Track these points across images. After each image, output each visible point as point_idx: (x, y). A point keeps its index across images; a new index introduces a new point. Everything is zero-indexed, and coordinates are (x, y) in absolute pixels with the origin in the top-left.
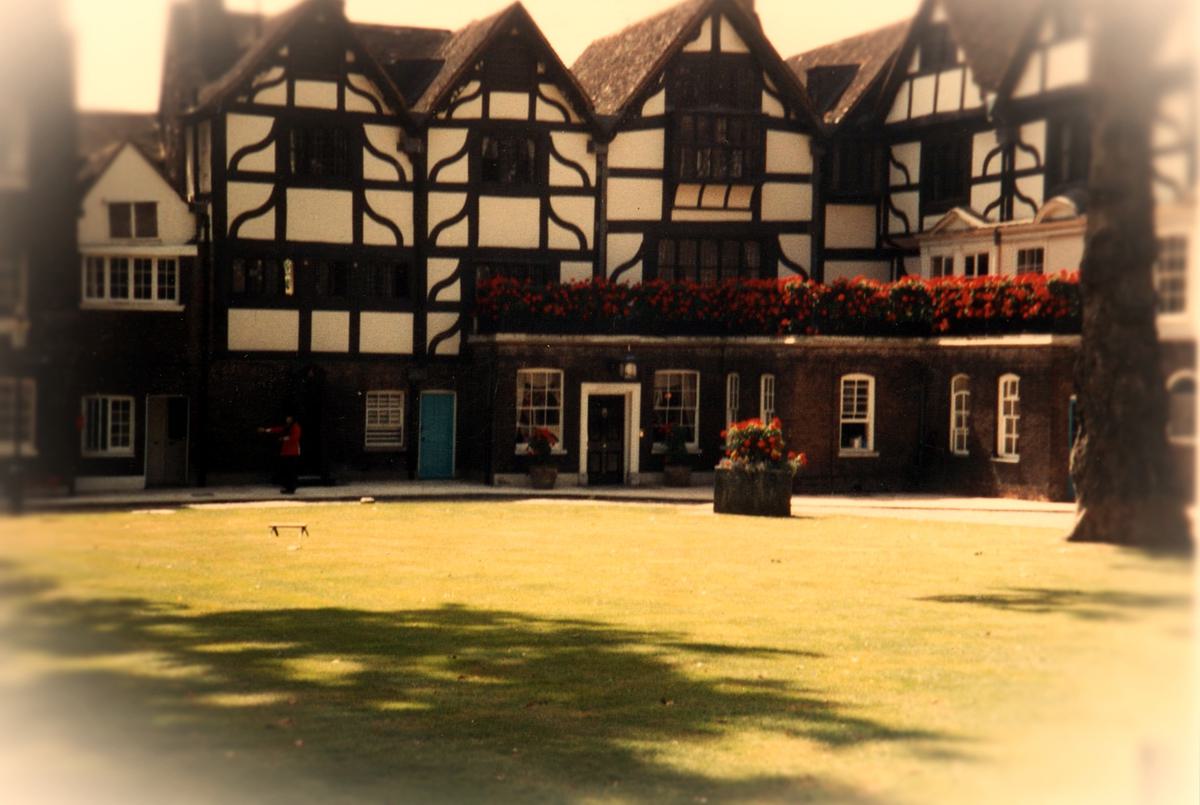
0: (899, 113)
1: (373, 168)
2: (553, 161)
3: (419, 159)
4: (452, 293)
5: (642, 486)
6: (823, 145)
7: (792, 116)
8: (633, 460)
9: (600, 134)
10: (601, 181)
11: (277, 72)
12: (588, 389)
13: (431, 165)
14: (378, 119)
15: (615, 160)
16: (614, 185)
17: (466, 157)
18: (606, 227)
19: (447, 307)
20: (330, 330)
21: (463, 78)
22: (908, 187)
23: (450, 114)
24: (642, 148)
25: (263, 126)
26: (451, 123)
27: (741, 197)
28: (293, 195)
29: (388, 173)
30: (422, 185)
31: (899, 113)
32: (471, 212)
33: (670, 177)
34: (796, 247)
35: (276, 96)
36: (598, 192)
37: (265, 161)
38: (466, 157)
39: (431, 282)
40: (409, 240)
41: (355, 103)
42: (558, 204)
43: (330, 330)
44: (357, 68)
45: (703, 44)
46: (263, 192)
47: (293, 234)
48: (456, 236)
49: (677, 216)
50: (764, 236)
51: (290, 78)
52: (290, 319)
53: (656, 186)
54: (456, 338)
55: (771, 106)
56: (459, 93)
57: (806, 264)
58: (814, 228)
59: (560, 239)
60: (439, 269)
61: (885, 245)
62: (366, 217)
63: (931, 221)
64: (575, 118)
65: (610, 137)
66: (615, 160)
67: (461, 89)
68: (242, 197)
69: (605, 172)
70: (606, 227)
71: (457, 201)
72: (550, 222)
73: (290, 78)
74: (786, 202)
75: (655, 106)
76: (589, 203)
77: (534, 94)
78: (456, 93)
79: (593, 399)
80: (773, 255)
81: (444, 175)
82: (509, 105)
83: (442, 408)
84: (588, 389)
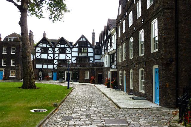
1: (49, 52)
3: (54, 51)
4: (57, 63)
6: (94, 49)
8: (71, 80)
9: (71, 49)
12: (66, 72)
13: (55, 51)
18: (72, 57)
19: (56, 64)
20: (45, 66)
21: (58, 43)
24: (75, 50)
25: (40, 48)
26: (57, 48)
29: (51, 52)
30: (54, 53)
32: (59, 55)
34: (92, 59)
35: (41, 46)
36: (71, 54)
37: (40, 51)
40: (53, 58)
41: (48, 46)
43: (45, 66)
45: (82, 40)
46: (40, 54)
48: (57, 58)
50: (88, 58)
51: (42, 44)
55: (89, 46)
58: (94, 57)
60: (55, 61)
68: (37, 55)
69: (72, 52)
70: (72, 57)
73: (42, 44)
74: (90, 55)
75: (77, 46)
77: (65, 45)
80: (89, 59)
81: (56, 52)
82: (63, 46)
83: (55, 74)
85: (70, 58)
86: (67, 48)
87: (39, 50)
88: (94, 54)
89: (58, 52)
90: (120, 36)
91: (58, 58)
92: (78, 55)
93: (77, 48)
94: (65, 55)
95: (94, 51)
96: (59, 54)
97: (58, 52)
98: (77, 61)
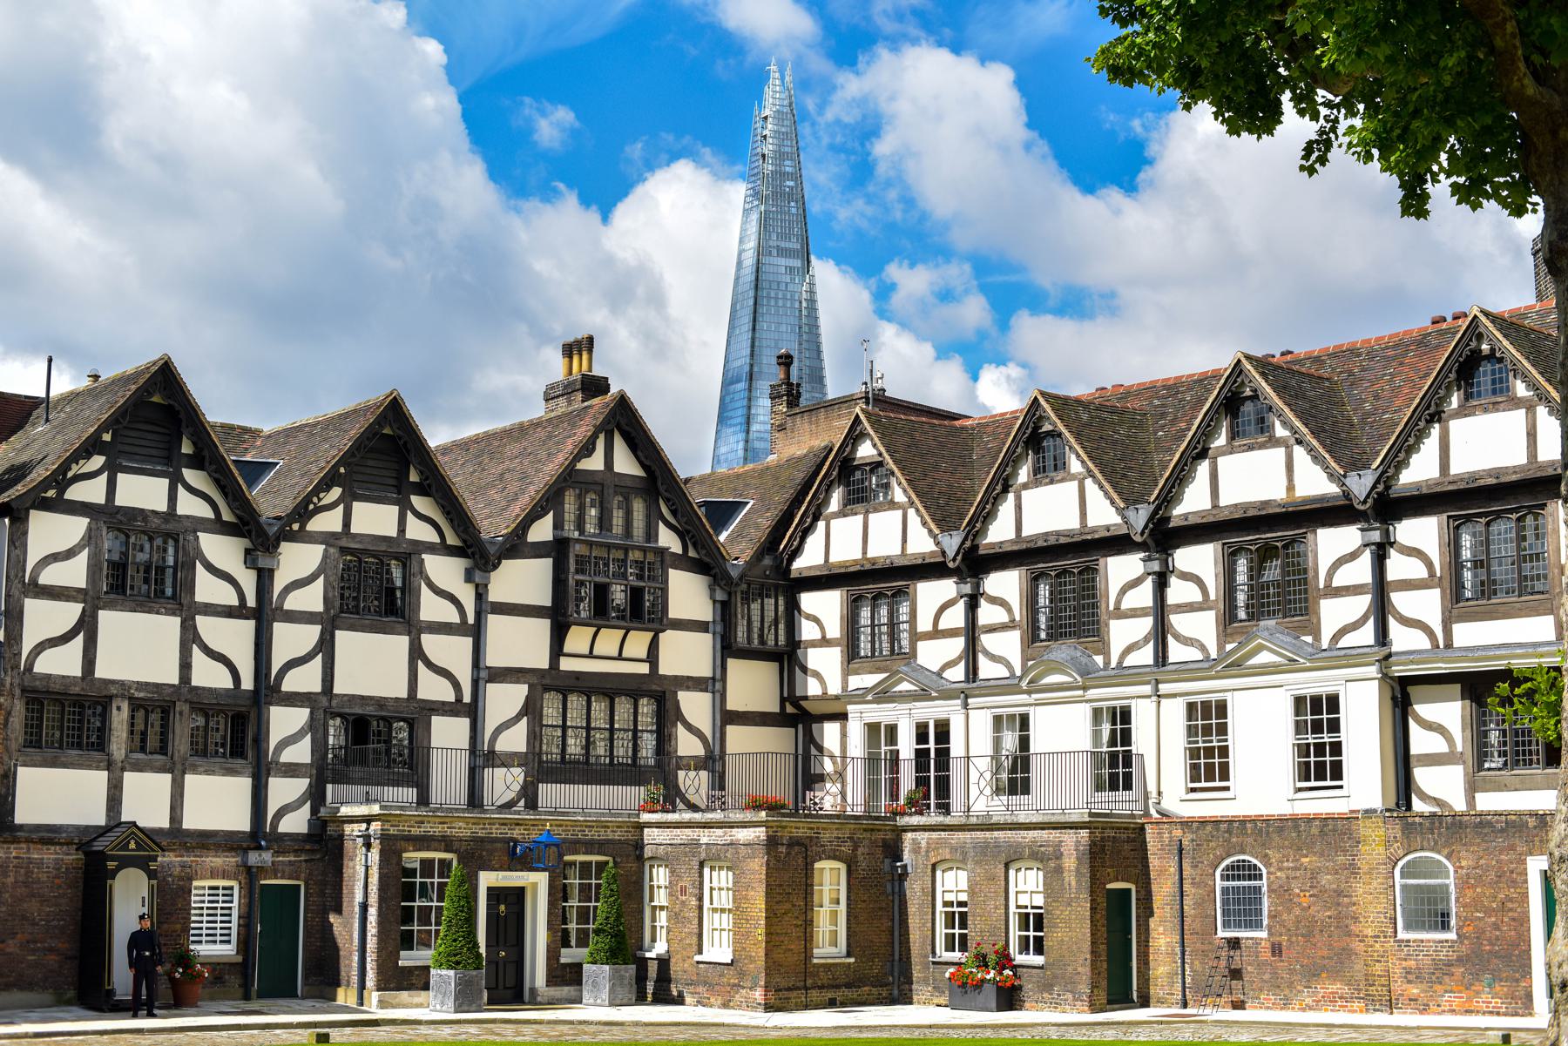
0: (810, 558)
1: (208, 589)
2: (424, 587)
3: (265, 578)
5: (552, 1003)
7: (692, 553)
10: (479, 614)
11: (98, 461)
13: (279, 584)
14: (219, 526)
15: (496, 594)
16: (494, 622)
17: (321, 579)
18: (485, 675)
19: (292, 770)
21: (325, 485)
22: (825, 642)
23: (302, 527)
27: (638, 643)
28: (106, 618)
29: (229, 597)
31: (810, 558)
32: (326, 646)
33: (559, 619)
34: (696, 707)
35: (91, 491)
36: (476, 633)
37: (74, 573)
38: (321, 579)
39: (274, 740)
40: (247, 683)
41: (189, 506)
42: (429, 642)
44: (197, 462)
45: (595, 463)
47: (100, 672)
48: (306, 679)
49: (566, 664)
51: (112, 469)
52: (94, 781)
53: (543, 627)
54: (305, 811)
56: (320, 500)
57: (707, 730)
58: (714, 685)
59: (433, 689)
60: (284, 722)
61: (790, 709)
62: (197, 654)
63: (859, 681)
64: (452, 540)
65: (495, 567)
66: (496, 594)
67: (322, 495)
71: (310, 635)
72: (421, 665)
73: (112, 469)
75: (542, 531)
76: (467, 642)
77: (405, 507)
78: (315, 500)
79: (495, 894)
80: (668, 718)
81: (293, 602)
84: (488, 879)
85: (456, 685)
86: (431, 548)
87: (69, 554)
88: (728, 648)
89: (319, 607)
90: (598, 441)
91: (316, 686)
92: (557, 650)
93: (544, 566)
94: (402, 642)
95: (725, 611)
96: (330, 622)
97: (319, 607)
98: (534, 736)
